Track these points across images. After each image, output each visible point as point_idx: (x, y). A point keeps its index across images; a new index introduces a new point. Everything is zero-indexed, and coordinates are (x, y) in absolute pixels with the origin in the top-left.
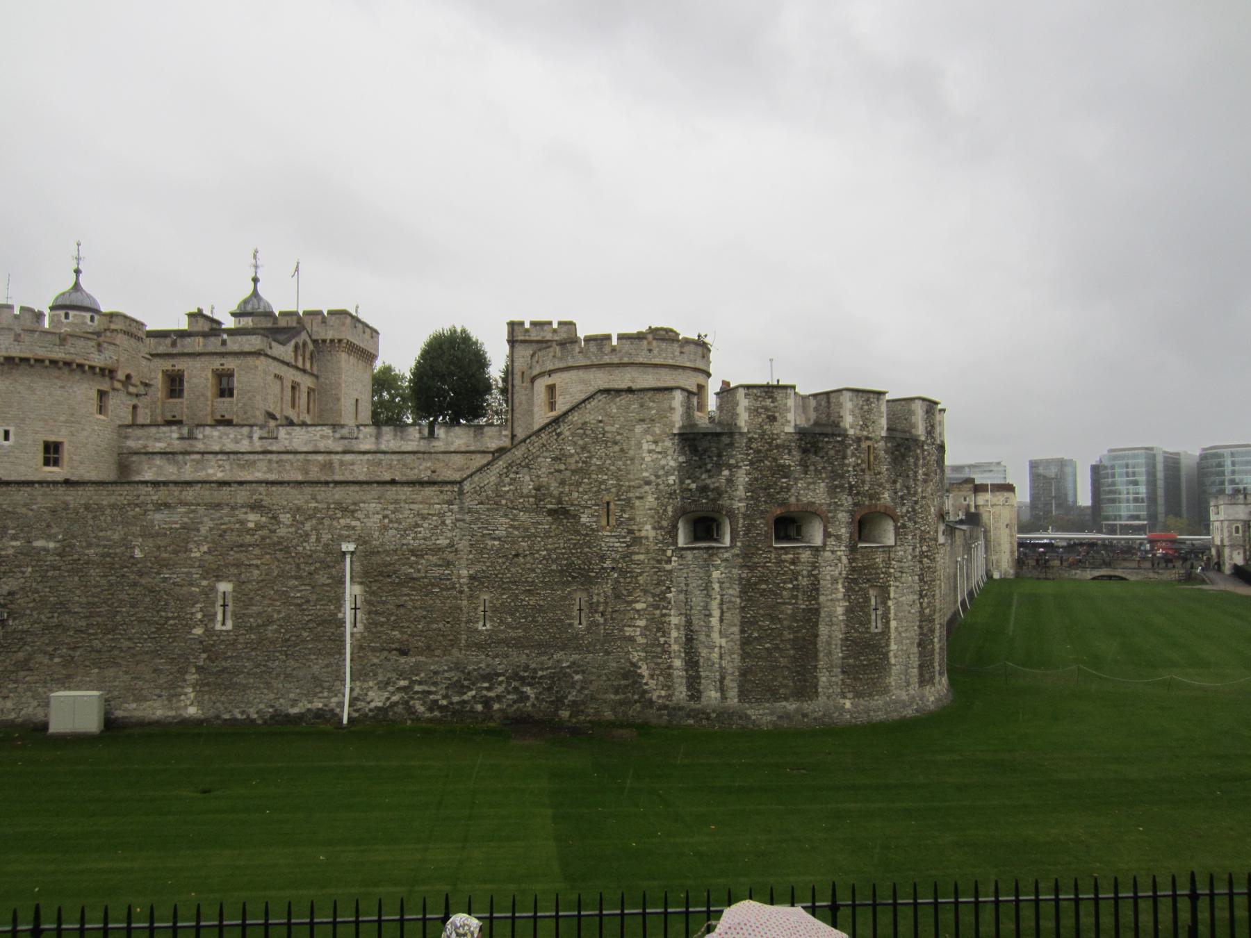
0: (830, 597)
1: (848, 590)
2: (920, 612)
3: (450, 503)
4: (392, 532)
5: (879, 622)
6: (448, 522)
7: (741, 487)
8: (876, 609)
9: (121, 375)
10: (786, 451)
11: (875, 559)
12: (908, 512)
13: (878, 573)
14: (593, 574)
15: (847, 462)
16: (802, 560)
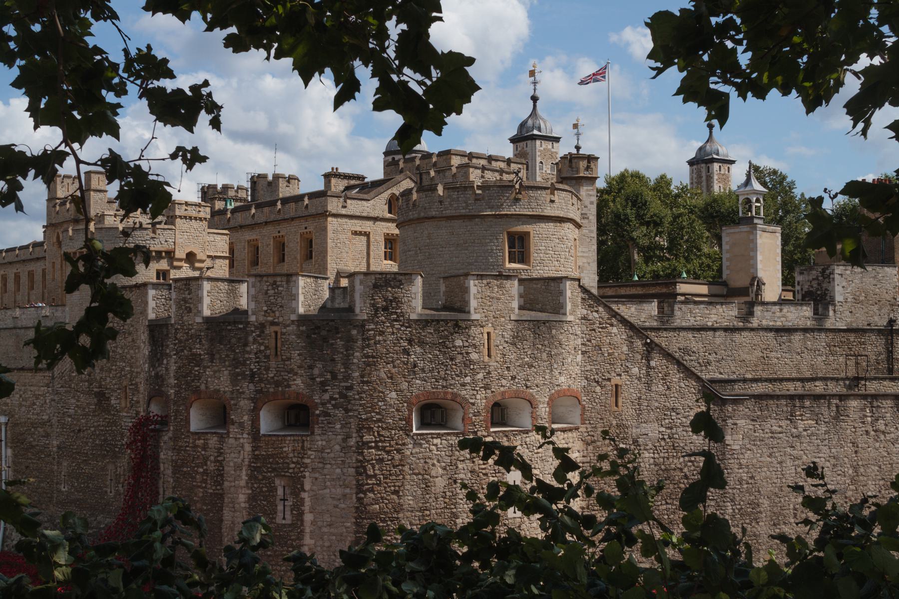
0: (233, 484)
1: (251, 477)
2: (357, 508)
3: (47, 386)
4: (23, 409)
5: (288, 513)
6: (48, 401)
7: (172, 375)
8: (284, 500)
9: (180, 254)
10: (198, 340)
11: (282, 448)
12: (332, 398)
13: (287, 463)
14: (117, 450)
15: (248, 349)
16: (210, 446)
